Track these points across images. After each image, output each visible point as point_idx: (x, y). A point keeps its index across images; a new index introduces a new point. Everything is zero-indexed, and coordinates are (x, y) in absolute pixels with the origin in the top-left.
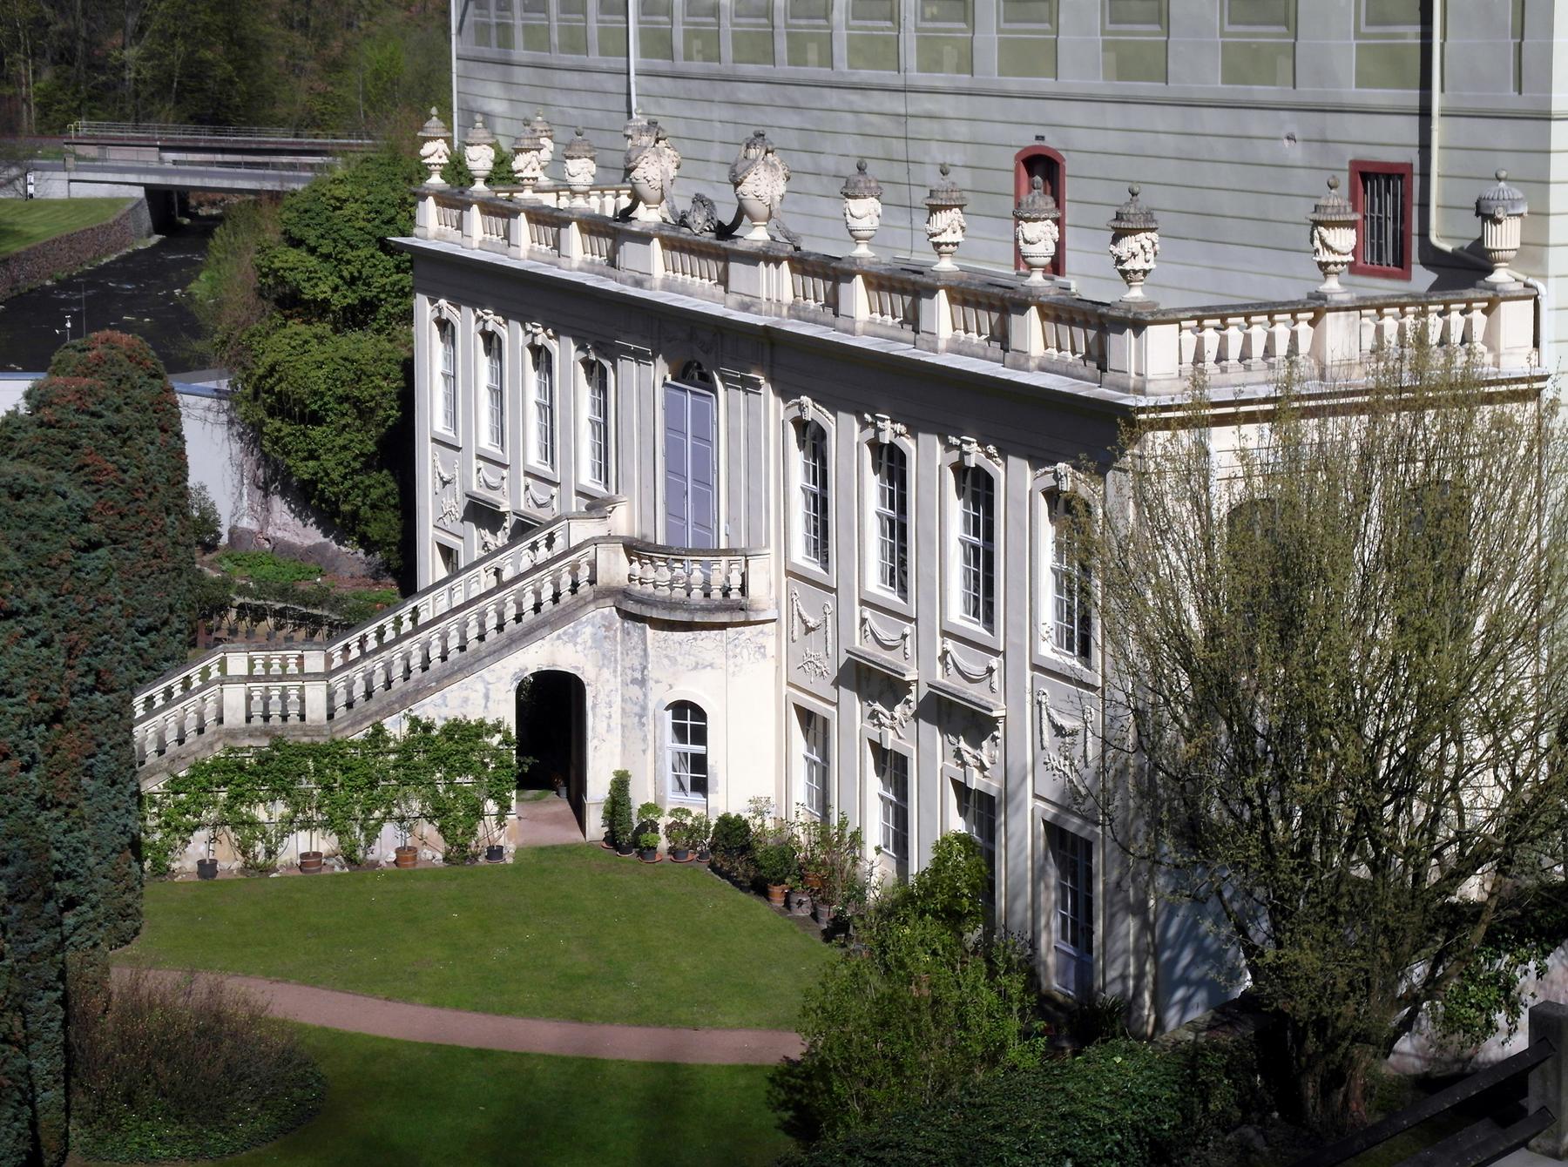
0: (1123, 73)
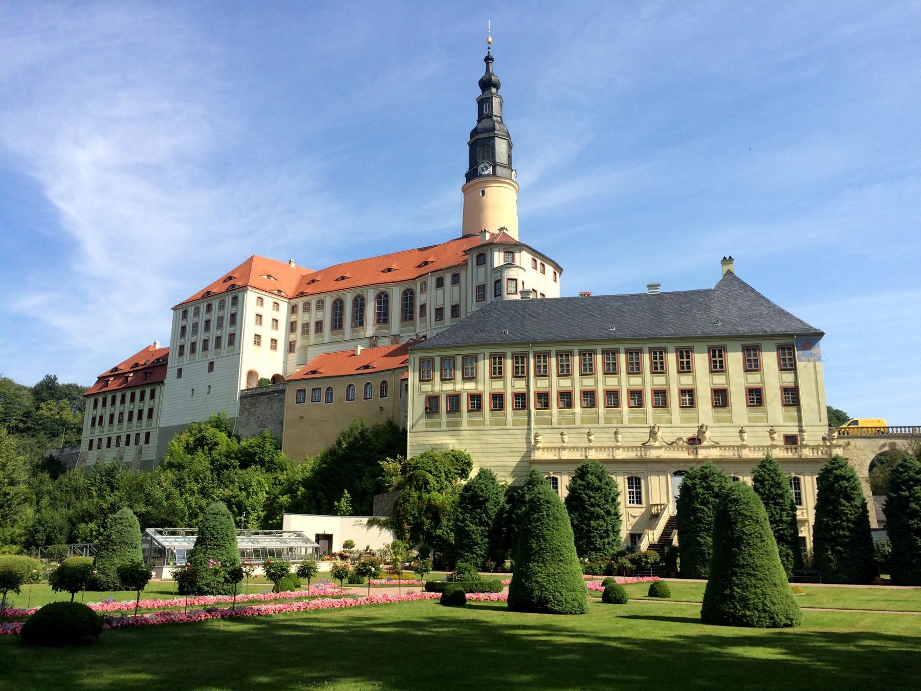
0: (718, 422)
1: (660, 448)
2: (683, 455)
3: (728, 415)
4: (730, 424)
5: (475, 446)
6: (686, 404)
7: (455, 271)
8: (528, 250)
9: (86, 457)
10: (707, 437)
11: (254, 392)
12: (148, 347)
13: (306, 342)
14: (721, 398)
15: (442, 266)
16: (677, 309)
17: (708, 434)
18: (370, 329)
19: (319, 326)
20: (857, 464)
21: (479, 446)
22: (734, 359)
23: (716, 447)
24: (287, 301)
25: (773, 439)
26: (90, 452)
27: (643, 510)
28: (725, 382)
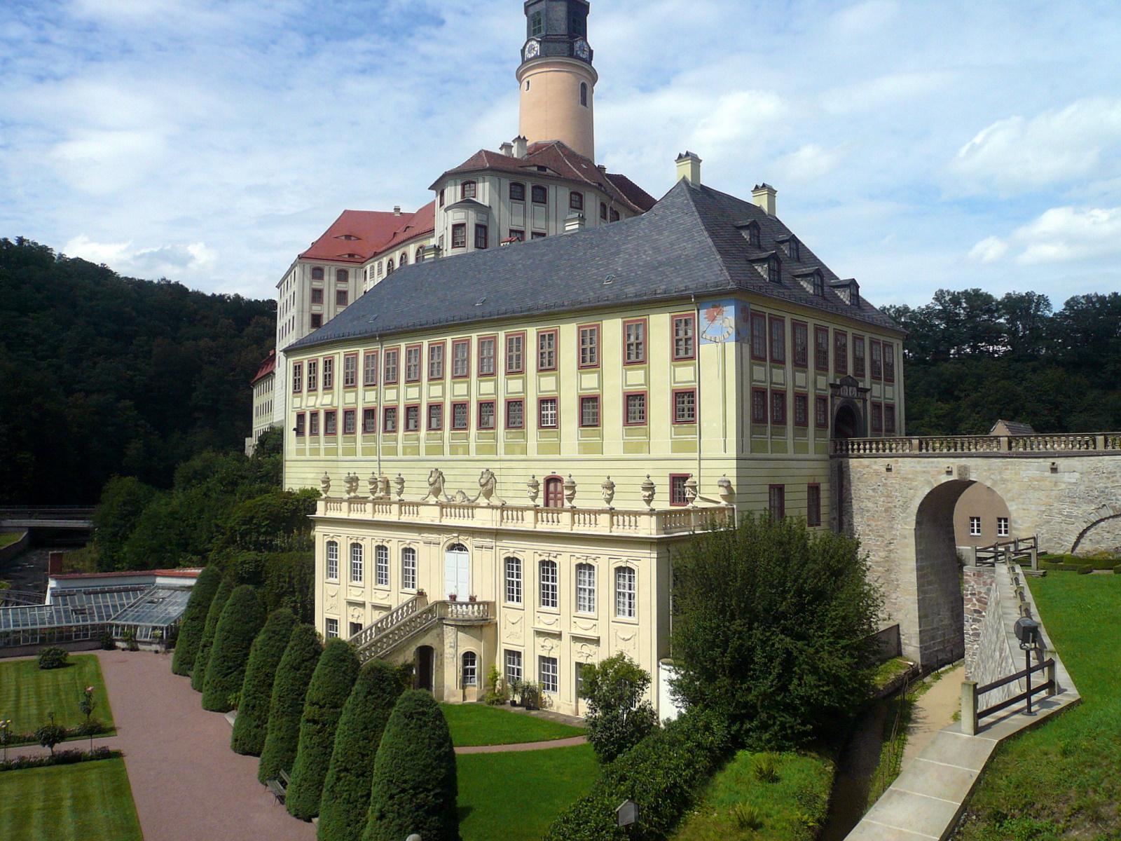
4: (599, 456)
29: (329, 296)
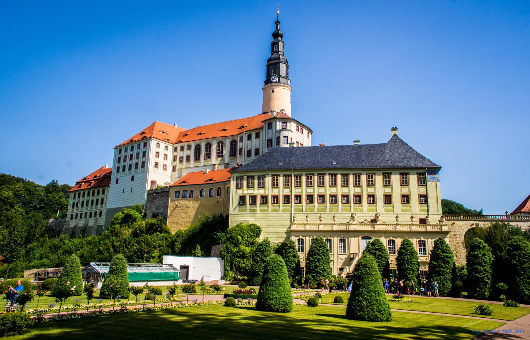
0: (386, 212)
1: (356, 224)
2: (369, 228)
3: (391, 208)
4: (392, 213)
5: (264, 222)
6: (371, 202)
7: (257, 131)
8: (294, 121)
9: (69, 224)
10: (379, 219)
11: (154, 192)
12: (102, 167)
13: (181, 167)
14: (388, 199)
15: (251, 128)
16: (368, 153)
17: (380, 217)
18: (214, 160)
19: (188, 158)
20: (458, 234)
21: (265, 222)
22: (396, 179)
23: (384, 225)
24: (172, 145)
25: (412, 221)
26: (71, 220)
27: (347, 256)
28: (390, 192)
29: (162, 156)
